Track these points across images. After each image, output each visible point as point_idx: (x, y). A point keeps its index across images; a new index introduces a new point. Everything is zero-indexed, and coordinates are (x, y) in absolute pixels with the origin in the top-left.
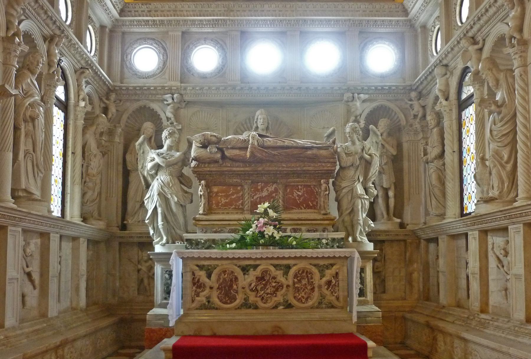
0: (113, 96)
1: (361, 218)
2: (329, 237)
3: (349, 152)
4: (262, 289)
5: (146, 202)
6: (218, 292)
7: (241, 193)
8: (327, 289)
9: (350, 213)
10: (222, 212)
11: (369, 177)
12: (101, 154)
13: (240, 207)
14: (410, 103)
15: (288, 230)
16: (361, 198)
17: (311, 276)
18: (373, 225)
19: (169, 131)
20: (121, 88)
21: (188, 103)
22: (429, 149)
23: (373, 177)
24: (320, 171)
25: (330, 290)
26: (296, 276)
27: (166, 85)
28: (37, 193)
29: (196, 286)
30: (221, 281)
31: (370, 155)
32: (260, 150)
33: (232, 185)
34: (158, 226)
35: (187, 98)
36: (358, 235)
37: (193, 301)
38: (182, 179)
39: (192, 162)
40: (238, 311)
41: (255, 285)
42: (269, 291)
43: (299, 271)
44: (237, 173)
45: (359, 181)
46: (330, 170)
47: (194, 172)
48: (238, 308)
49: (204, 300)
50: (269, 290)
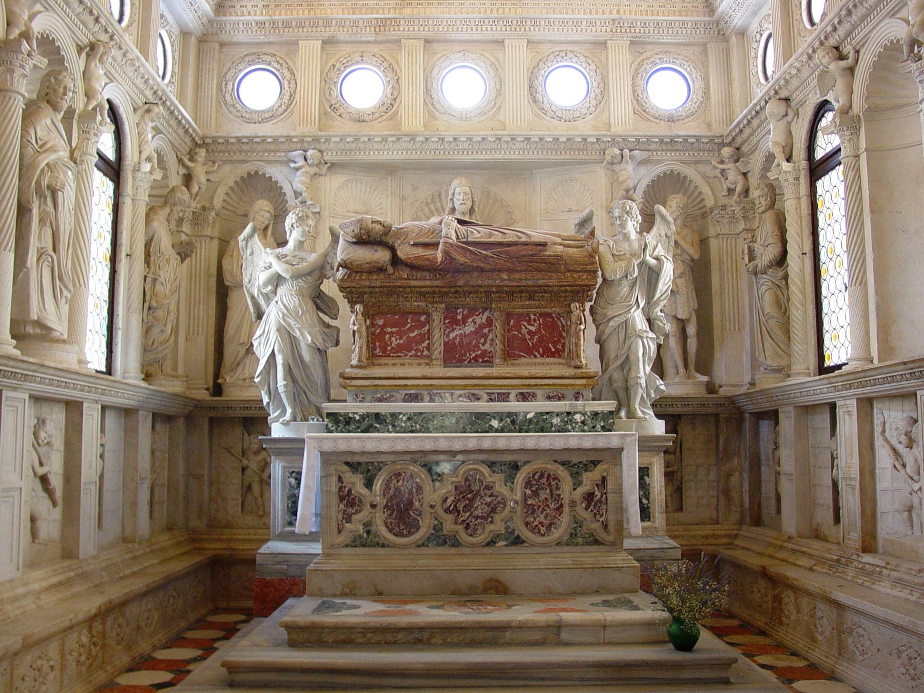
0: (202, 152)
1: (642, 374)
2: (586, 410)
3: (620, 253)
4: (467, 508)
5: (255, 344)
6: (386, 515)
7: (427, 328)
9: (622, 366)
10: (393, 362)
11: (655, 298)
12: (179, 258)
13: (424, 354)
14: (722, 166)
15: (512, 396)
16: (641, 338)
17: (557, 483)
18: (663, 387)
19: (297, 215)
20: (215, 140)
21: (333, 167)
22: (757, 247)
23: (662, 298)
24: (568, 288)
25: (592, 511)
26: (528, 484)
27: (292, 134)
28: (60, 327)
29: (345, 502)
30: (391, 492)
31: (656, 259)
32: (462, 248)
33: (410, 313)
34: (277, 388)
35: (328, 157)
36: (637, 406)
37: (340, 531)
38: (321, 302)
39: (338, 270)
40: (424, 550)
41: (454, 501)
42: (478, 513)
43: (534, 475)
44: (418, 289)
45: (638, 306)
46: (586, 286)
47: (342, 289)
48: (423, 544)
49: (361, 529)
50: (480, 511)
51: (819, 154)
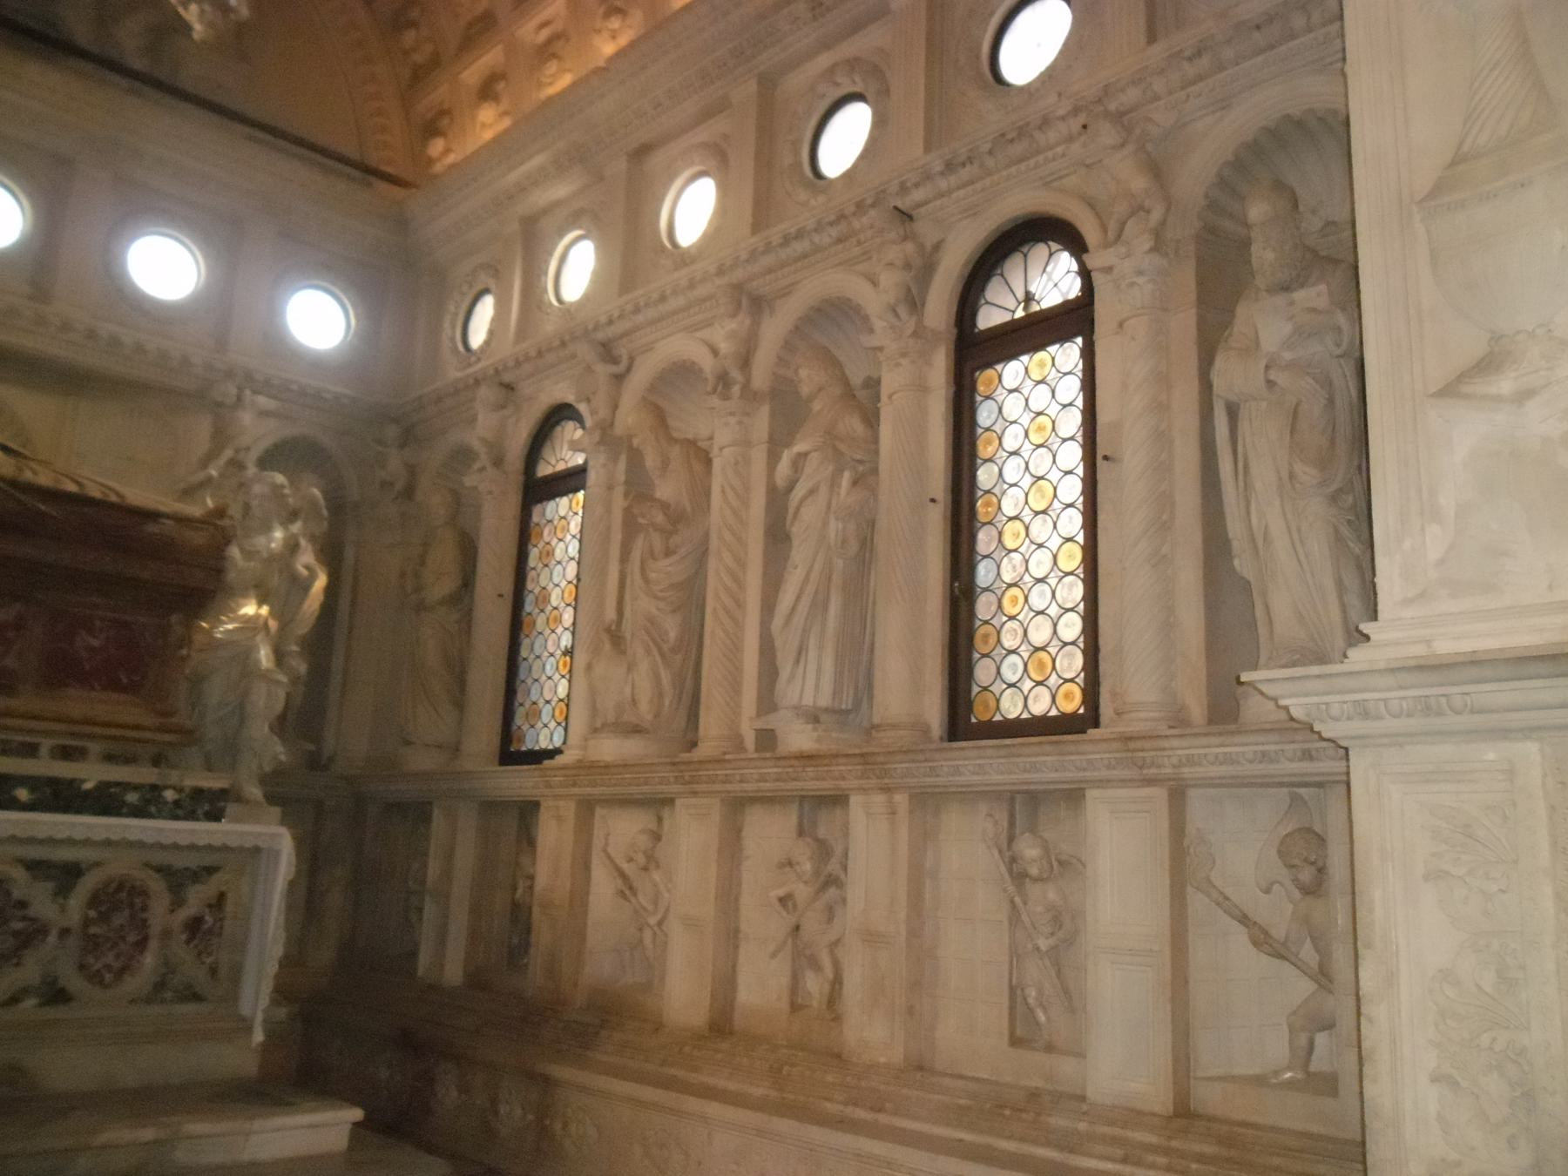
8: (188, 942)
15: (44, 751)
25: (196, 946)
26: (94, 900)
51: (544, 470)
